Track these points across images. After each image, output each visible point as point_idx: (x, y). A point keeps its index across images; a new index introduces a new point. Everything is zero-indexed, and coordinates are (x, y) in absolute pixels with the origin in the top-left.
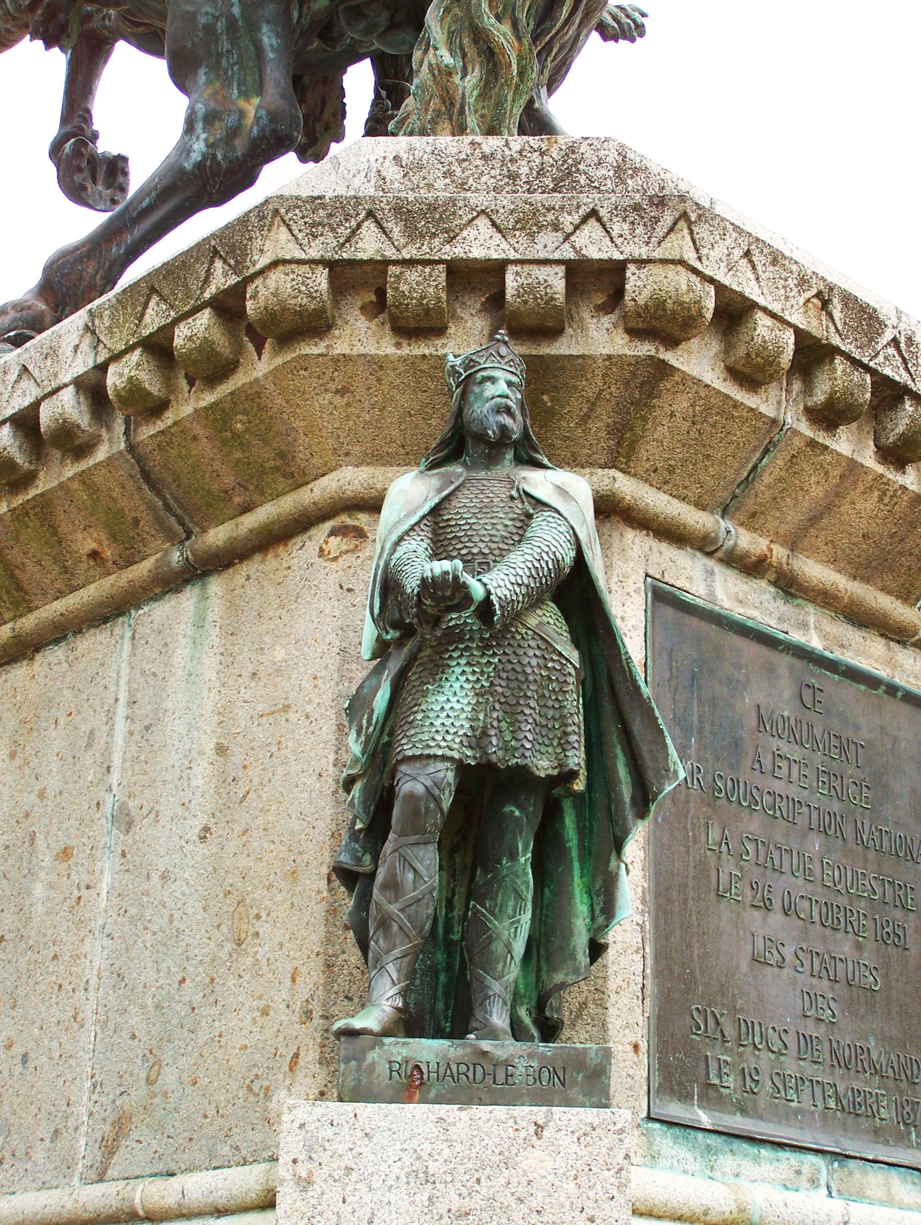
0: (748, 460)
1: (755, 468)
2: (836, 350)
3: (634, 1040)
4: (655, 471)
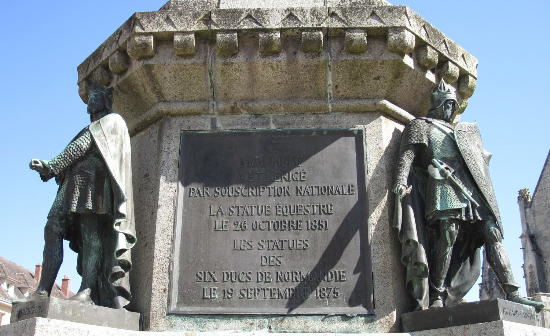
0: (206, 80)
1: (211, 80)
2: (216, 31)
4: (176, 96)
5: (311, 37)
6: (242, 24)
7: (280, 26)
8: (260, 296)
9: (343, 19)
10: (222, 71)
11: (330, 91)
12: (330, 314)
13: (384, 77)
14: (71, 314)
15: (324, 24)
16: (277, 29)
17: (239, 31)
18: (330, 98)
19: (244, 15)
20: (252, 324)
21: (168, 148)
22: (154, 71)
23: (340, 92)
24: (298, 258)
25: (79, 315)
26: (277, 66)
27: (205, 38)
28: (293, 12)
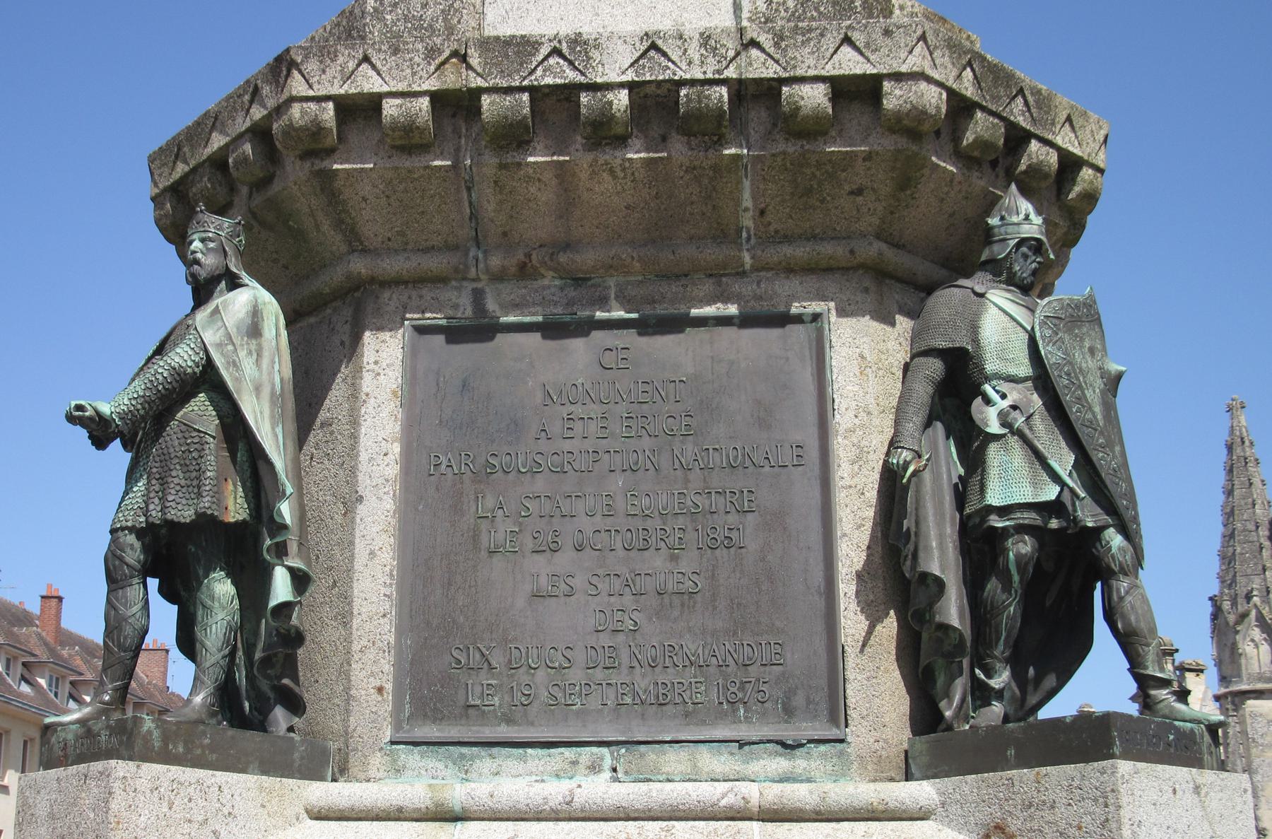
1: (471, 203)
2: (480, 91)
3: (378, 684)
5: (700, 102)
6: (539, 72)
7: (630, 76)
8: (594, 703)
9: (777, 56)
10: (495, 182)
11: (748, 221)
12: (747, 739)
13: (873, 189)
14: (181, 750)
15: (732, 68)
16: (622, 85)
17: (532, 90)
18: (749, 239)
19: (544, 51)
20: (575, 763)
21: (376, 363)
22: (338, 184)
23: (770, 224)
24: (676, 613)
25: (199, 751)
26: (624, 170)
27: (455, 106)
28: (660, 43)
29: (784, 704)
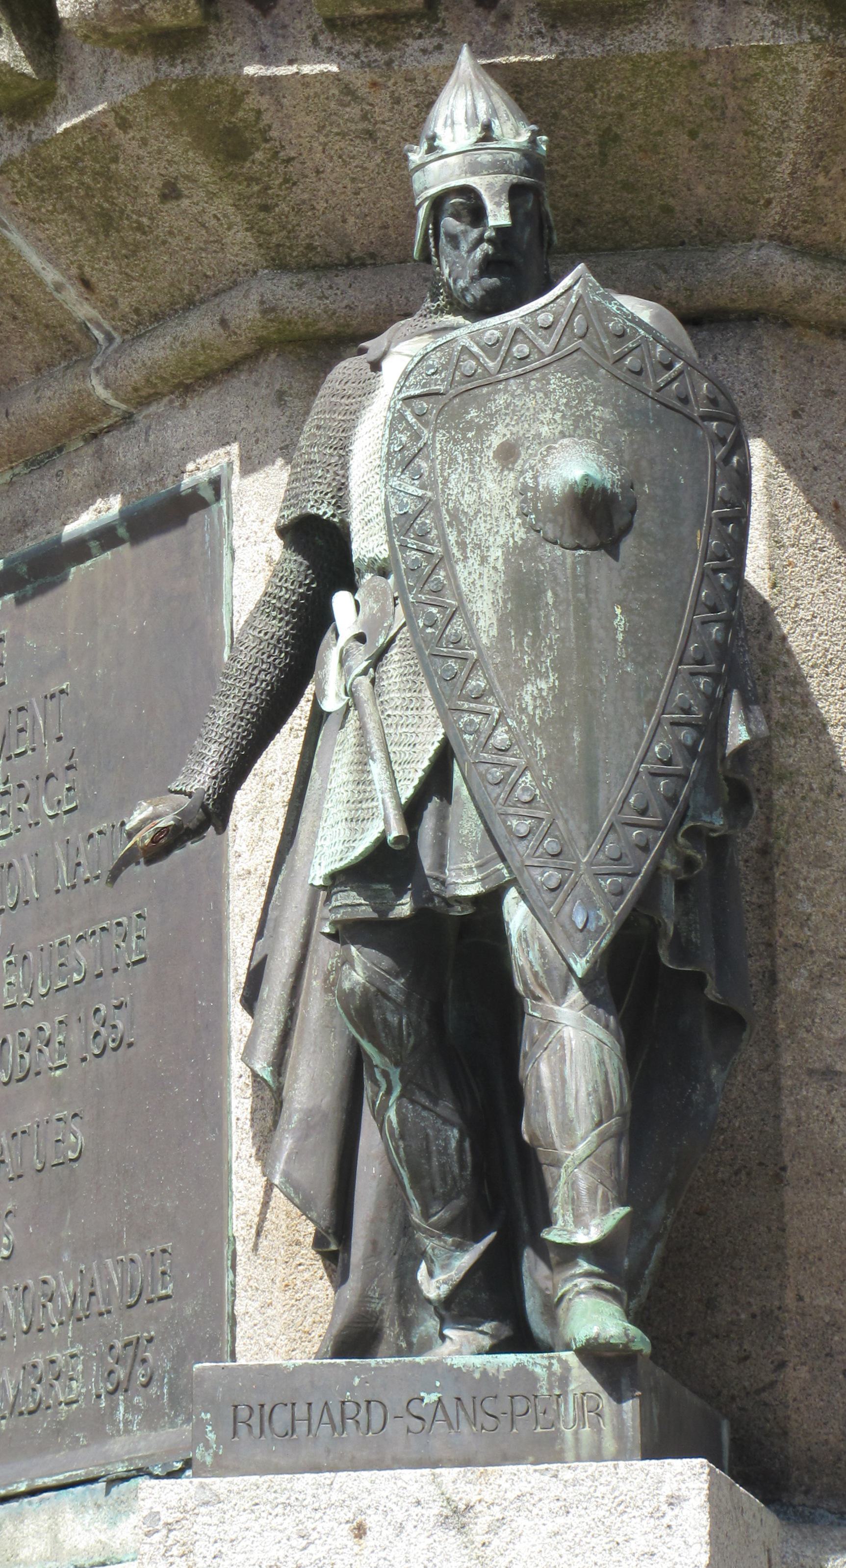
11: (84, 310)
13: (187, 177)
18: (110, 339)
29: (171, 1385)
